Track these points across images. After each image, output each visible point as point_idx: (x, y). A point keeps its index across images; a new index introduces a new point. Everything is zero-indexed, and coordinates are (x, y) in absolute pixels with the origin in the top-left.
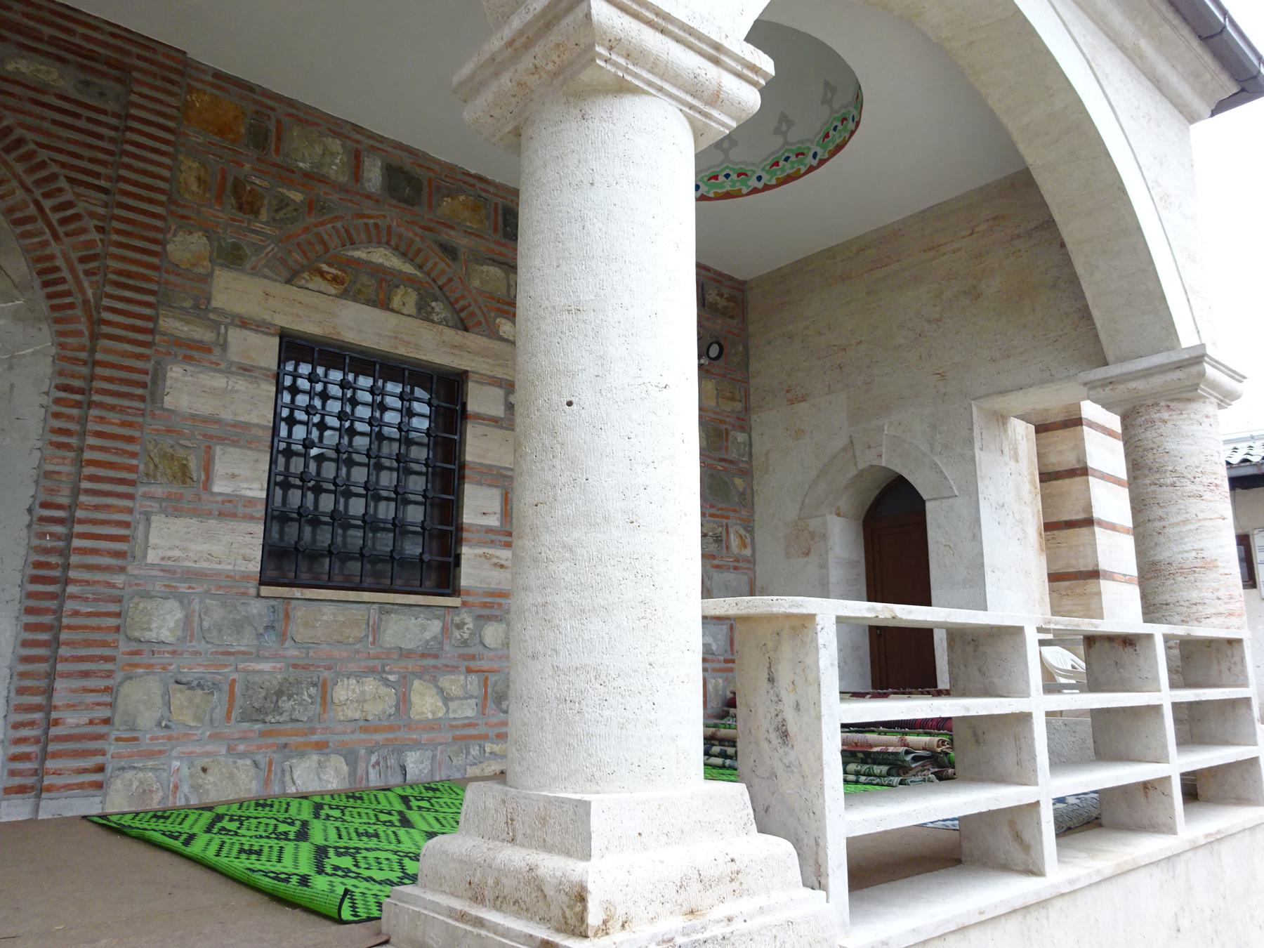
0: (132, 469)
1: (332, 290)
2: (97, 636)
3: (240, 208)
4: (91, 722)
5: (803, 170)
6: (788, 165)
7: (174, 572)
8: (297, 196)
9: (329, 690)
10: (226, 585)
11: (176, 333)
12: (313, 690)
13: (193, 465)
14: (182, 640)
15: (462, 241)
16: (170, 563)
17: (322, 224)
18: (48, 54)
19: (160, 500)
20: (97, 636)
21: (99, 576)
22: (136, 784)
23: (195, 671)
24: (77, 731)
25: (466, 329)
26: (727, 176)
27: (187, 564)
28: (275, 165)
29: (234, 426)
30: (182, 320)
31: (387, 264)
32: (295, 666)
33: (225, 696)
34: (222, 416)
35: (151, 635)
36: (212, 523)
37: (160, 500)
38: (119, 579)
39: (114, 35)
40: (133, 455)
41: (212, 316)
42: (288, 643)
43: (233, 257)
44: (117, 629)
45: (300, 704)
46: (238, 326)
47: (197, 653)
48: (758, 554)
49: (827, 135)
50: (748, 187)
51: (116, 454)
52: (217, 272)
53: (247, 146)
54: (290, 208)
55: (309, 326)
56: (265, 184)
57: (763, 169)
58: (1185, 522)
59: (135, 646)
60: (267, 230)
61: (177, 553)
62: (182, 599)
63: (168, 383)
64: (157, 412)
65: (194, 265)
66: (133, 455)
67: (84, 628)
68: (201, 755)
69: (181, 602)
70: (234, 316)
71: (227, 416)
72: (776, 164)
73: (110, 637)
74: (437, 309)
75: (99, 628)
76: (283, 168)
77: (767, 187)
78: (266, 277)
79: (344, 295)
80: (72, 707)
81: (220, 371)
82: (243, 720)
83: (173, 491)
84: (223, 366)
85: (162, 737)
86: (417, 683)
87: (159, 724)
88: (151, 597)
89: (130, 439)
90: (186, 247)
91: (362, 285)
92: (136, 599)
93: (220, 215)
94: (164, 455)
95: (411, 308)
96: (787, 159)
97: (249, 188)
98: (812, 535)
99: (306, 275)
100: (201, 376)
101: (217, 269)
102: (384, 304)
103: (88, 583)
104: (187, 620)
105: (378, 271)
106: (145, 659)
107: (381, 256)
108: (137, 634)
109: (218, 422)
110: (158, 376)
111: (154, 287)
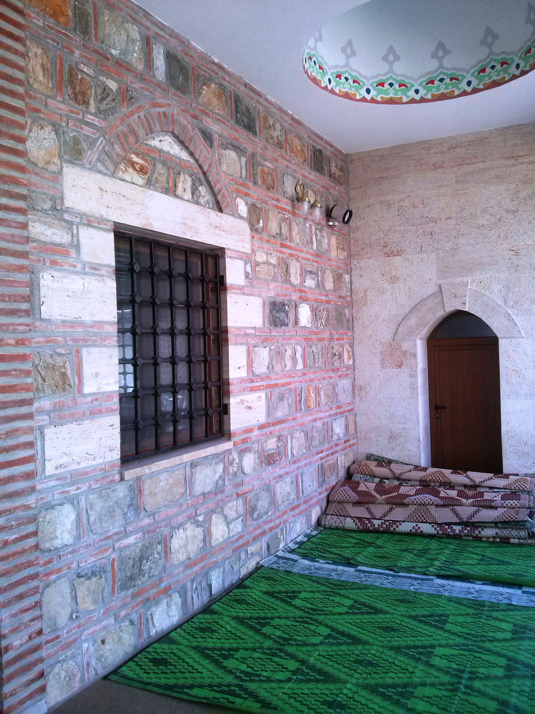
0: (27, 388)
1: (139, 180)
2: (23, 559)
3: (76, 99)
4: (30, 638)
5: (457, 93)
6: (443, 85)
7: (65, 478)
8: (113, 85)
9: (168, 543)
10: (101, 479)
11: (43, 238)
12: (159, 547)
13: (69, 372)
14: (78, 538)
15: (215, 128)
16: (62, 470)
17: (132, 113)
19: (48, 413)
20: (23, 559)
21: (18, 502)
22: (63, 674)
23: (89, 561)
24: (22, 649)
25: (221, 210)
26: (391, 85)
27: (74, 467)
28: (96, 51)
29: (92, 327)
30: (45, 223)
31: (172, 152)
32: (148, 532)
33: (110, 575)
34: (83, 319)
35: (57, 543)
36: (87, 424)
37: (48, 413)
38: (31, 500)
40: (28, 373)
41: (66, 216)
42: (143, 513)
43: (74, 153)
44: (36, 546)
45: (154, 562)
46: (85, 225)
47: (89, 545)
48: (357, 362)
49: (483, 70)
50: (408, 97)
51: (16, 376)
52: (65, 169)
53: (75, 30)
54: (109, 98)
55: (133, 220)
56: (91, 72)
57: (420, 85)
59: (46, 557)
60: (96, 121)
61: (65, 460)
62: (73, 501)
63: (43, 291)
64: (38, 324)
65: (48, 163)
66: (28, 373)
67: (14, 554)
68: (100, 631)
69: (72, 503)
70: (82, 215)
71: (87, 318)
72: (432, 82)
73: (32, 557)
74: (202, 193)
75: (24, 551)
76: (100, 54)
77: (423, 100)
78: (100, 172)
79: (149, 184)
80: (15, 630)
81: (76, 273)
82: (122, 590)
83: (57, 400)
84: (79, 267)
85: (75, 628)
86: (214, 517)
87: (71, 617)
88: (53, 507)
89: (23, 358)
90: (41, 143)
91: (159, 174)
92: (43, 513)
93: (62, 106)
94: (47, 367)
95: (188, 195)
96: (441, 80)
97: (80, 77)
98: (404, 353)
99: (122, 166)
100: (65, 280)
101: (64, 165)
102: (171, 190)
103: (9, 511)
104: (79, 517)
105: (167, 160)
106: (56, 564)
107: (167, 145)
108: (47, 545)
109: (82, 324)
110: (33, 285)
111: (23, 191)
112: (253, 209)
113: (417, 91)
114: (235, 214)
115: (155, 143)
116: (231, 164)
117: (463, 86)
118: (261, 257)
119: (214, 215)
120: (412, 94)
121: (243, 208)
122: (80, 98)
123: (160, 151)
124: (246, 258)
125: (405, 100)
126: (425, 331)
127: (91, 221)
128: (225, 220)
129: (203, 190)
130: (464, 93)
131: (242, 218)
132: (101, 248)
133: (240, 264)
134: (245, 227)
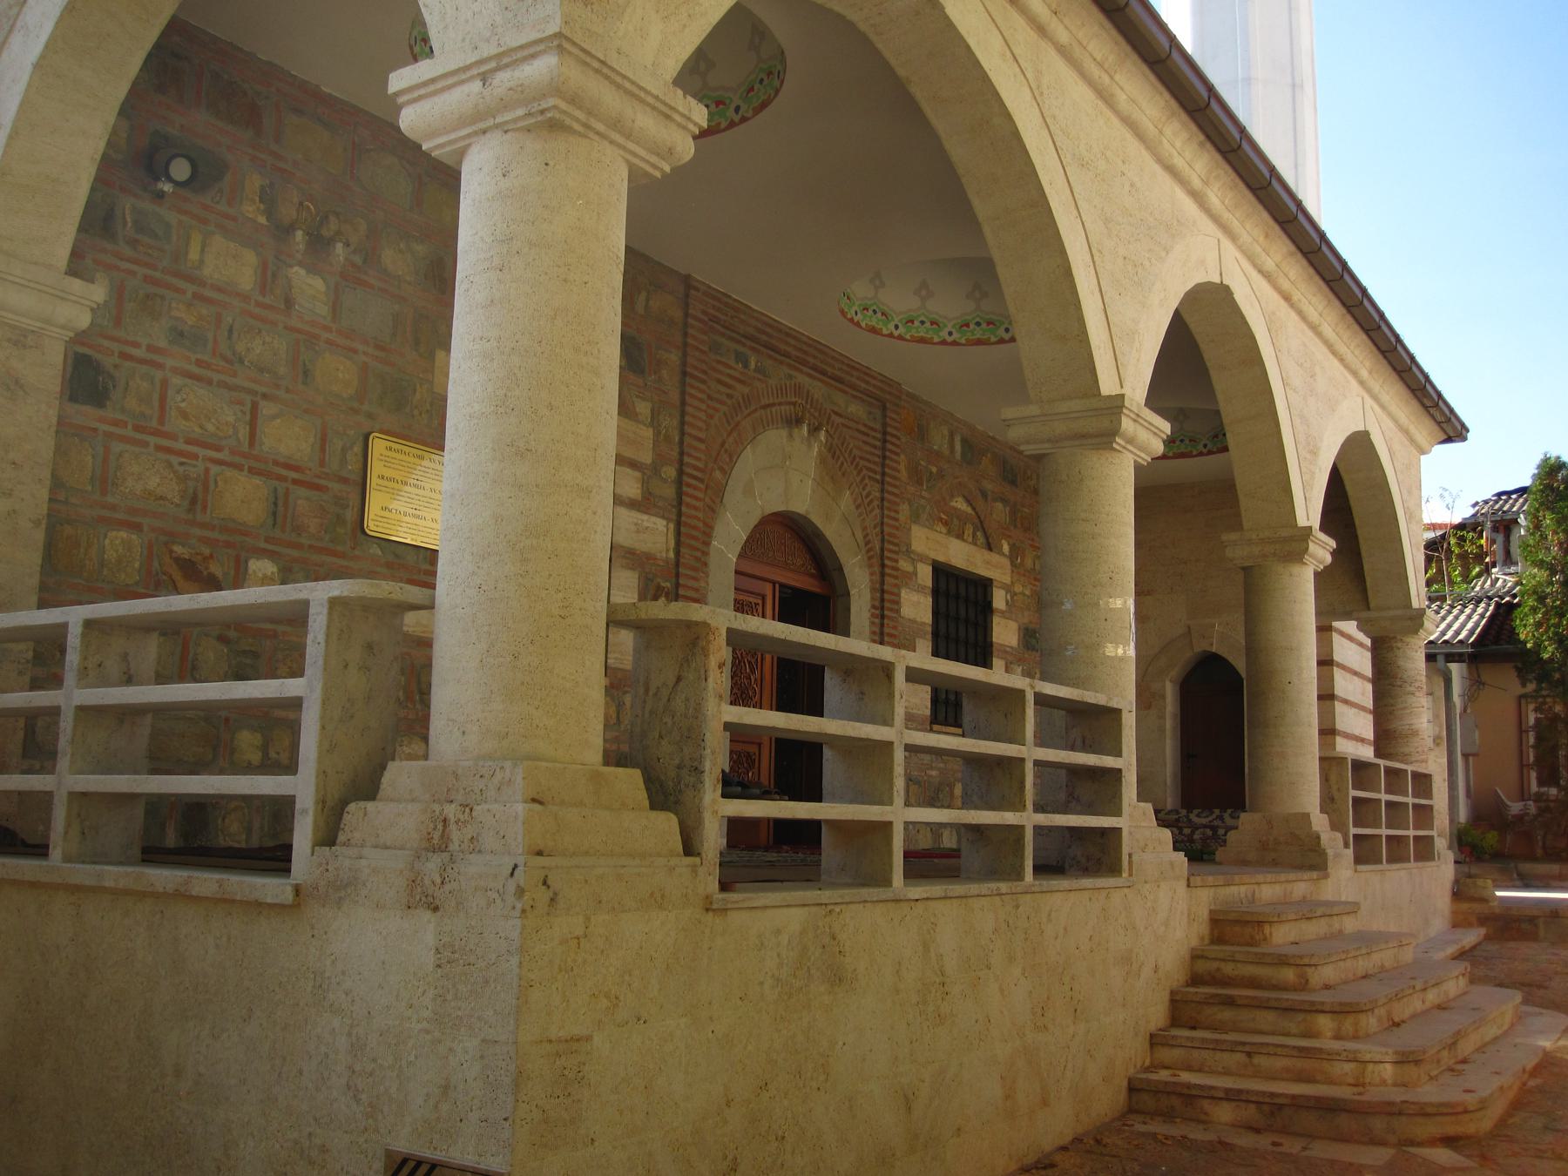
1: (944, 530)
8: (934, 470)
25: (990, 549)
43: (916, 517)
79: (949, 533)
102: (960, 536)
107: (960, 504)
112: (1012, 547)
114: (1001, 553)
115: (953, 504)
116: (999, 513)
117: (1200, 447)
118: (1018, 588)
119: (986, 552)
121: (1006, 548)
122: (919, 483)
123: (955, 509)
124: (1007, 588)
126: (1176, 672)
127: (923, 558)
128: (994, 557)
130: (1201, 454)
132: (925, 575)
133: (1003, 592)
134: (1006, 562)
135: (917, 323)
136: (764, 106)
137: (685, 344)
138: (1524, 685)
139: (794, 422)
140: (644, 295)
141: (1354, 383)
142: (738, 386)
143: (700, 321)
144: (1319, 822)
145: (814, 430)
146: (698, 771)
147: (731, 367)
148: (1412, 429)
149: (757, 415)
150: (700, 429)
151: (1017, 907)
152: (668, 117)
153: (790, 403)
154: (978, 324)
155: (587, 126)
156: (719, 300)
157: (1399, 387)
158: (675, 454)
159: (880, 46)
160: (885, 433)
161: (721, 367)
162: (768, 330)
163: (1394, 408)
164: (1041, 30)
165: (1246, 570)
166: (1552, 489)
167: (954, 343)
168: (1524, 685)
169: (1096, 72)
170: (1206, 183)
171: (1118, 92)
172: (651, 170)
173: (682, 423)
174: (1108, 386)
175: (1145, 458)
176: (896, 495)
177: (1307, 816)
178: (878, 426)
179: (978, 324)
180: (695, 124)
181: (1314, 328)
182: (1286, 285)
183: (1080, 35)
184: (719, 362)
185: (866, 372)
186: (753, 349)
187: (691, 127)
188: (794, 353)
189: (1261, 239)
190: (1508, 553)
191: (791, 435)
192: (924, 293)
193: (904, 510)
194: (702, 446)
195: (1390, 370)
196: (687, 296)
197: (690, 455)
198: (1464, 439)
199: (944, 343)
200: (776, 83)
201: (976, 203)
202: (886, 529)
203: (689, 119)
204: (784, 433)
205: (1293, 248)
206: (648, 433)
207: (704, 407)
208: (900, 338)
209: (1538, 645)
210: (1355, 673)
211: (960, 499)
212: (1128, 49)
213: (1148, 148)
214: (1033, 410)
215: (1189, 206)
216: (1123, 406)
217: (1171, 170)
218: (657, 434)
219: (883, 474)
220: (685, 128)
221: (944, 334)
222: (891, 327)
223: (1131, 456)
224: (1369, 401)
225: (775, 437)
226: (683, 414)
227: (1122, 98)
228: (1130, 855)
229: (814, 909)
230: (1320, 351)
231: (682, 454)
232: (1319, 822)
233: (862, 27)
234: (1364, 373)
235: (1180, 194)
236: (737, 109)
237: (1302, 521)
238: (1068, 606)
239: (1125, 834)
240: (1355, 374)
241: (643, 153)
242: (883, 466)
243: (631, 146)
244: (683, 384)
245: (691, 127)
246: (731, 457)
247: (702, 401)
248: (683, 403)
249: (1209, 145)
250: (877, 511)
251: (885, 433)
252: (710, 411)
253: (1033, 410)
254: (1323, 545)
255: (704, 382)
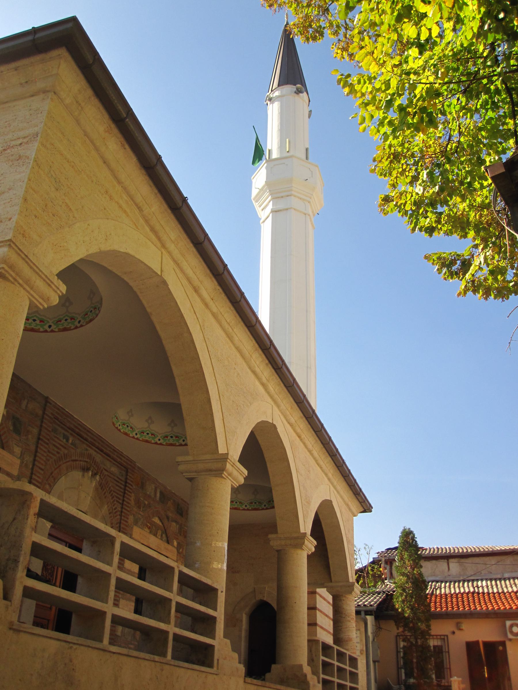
1: (148, 531)
8: (146, 503)
15: (170, 515)
18: (117, 465)
25: (168, 543)
26: (236, 502)
39: (127, 459)
43: (136, 523)
58: (346, 628)
77: (248, 510)
79: (150, 532)
95: (160, 537)
102: (155, 535)
107: (156, 520)
112: (179, 544)
113: (246, 506)
115: (153, 520)
116: (174, 527)
117: (263, 506)
119: (166, 544)
120: (244, 507)
121: (175, 543)
122: (139, 507)
123: (154, 522)
125: (241, 509)
126: (247, 610)
128: (170, 547)
129: (164, 535)
130: (263, 509)
131: (175, 547)
134: (175, 550)
135: (145, 434)
136: (91, 321)
137: (41, 426)
138: (398, 629)
139: (85, 470)
140: (26, 401)
141: (326, 479)
142: (63, 449)
143: (50, 417)
144: (307, 669)
145: (94, 475)
146: (16, 561)
147: (60, 440)
148: (350, 503)
149: (68, 464)
150: (42, 464)
151: (162, 670)
152: (49, 285)
153: (85, 461)
154: (172, 437)
155: (15, 280)
156: (58, 409)
157: (344, 484)
158: (28, 473)
159: (141, 298)
160: (126, 482)
161: (56, 439)
162: (79, 427)
163: (342, 493)
164: (206, 305)
165: (278, 551)
166: (407, 542)
167: (161, 444)
168: (398, 629)
169: (227, 326)
170: (268, 381)
171: (235, 336)
172: (39, 305)
173: (34, 460)
174: (222, 450)
175: (236, 485)
176: (128, 511)
177: (301, 667)
178: (123, 479)
179: (172, 437)
180: (61, 291)
181: (310, 451)
182: (299, 431)
183: (221, 310)
184: (56, 437)
185: (121, 454)
186: (71, 434)
187: (59, 292)
188: (90, 439)
189: (289, 409)
190: (391, 574)
191: (83, 476)
192: (150, 421)
193: (131, 518)
194: (42, 472)
195: (341, 476)
196: (46, 405)
197: (35, 475)
198: (371, 511)
199: (156, 443)
200: (97, 312)
201: (173, 367)
202: (122, 526)
203: (58, 288)
204: (81, 474)
205: (302, 415)
206: (18, 462)
207: (45, 455)
208: (137, 439)
209: (403, 610)
210: (326, 616)
211: (157, 518)
212: (240, 320)
213: (245, 362)
214: (189, 458)
215: (261, 389)
216: (227, 458)
217: (254, 372)
218: (22, 463)
219: (123, 501)
220: (56, 292)
221: (156, 440)
222: (134, 434)
223: (230, 482)
224: (331, 487)
225: (77, 474)
226: (35, 456)
227: (236, 339)
228: (218, 660)
229: (63, 644)
230: (312, 462)
231: (32, 473)
232: (307, 669)
233: (135, 289)
234: (330, 475)
235: (257, 383)
236: (79, 322)
237: (302, 530)
238: (198, 544)
239: (216, 649)
240: (326, 475)
241: (37, 297)
242: (124, 497)
243: (32, 292)
244: (38, 443)
245: (59, 292)
246: (54, 479)
247: (45, 452)
248: (36, 451)
249: (270, 365)
250: (119, 517)
251: (126, 482)
252: (48, 458)
253: (189, 458)
254: (311, 543)
255: (47, 444)
